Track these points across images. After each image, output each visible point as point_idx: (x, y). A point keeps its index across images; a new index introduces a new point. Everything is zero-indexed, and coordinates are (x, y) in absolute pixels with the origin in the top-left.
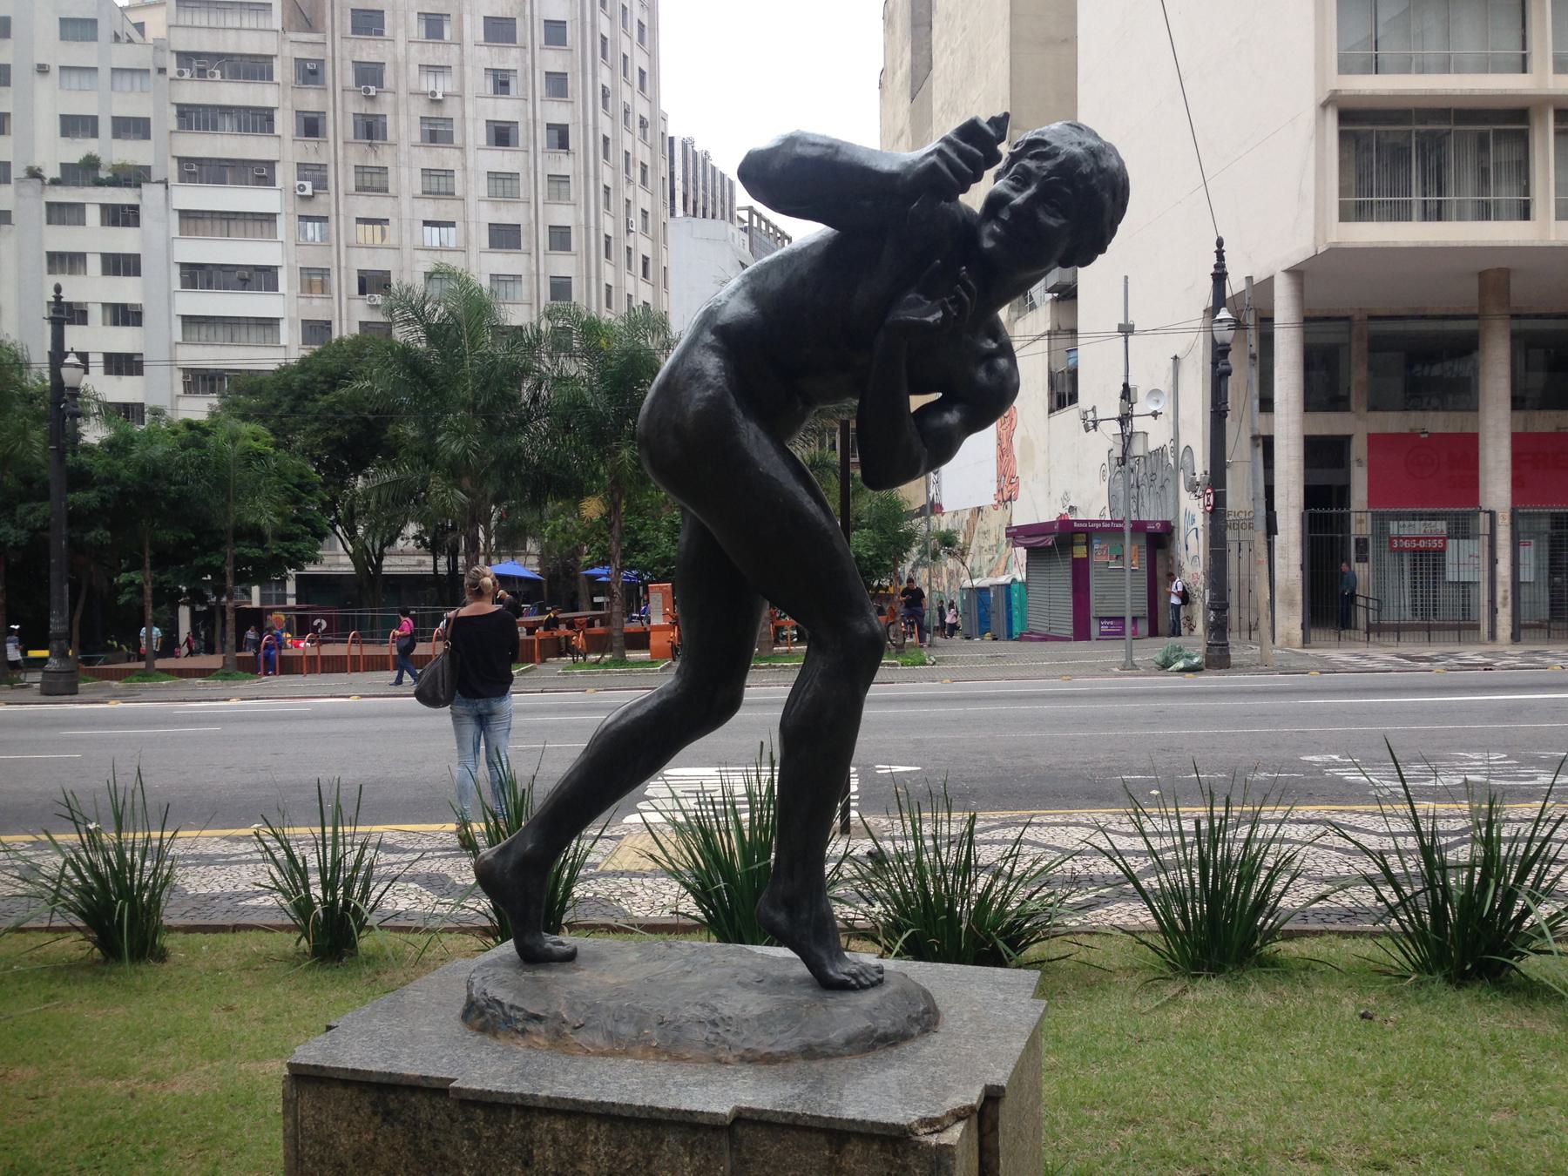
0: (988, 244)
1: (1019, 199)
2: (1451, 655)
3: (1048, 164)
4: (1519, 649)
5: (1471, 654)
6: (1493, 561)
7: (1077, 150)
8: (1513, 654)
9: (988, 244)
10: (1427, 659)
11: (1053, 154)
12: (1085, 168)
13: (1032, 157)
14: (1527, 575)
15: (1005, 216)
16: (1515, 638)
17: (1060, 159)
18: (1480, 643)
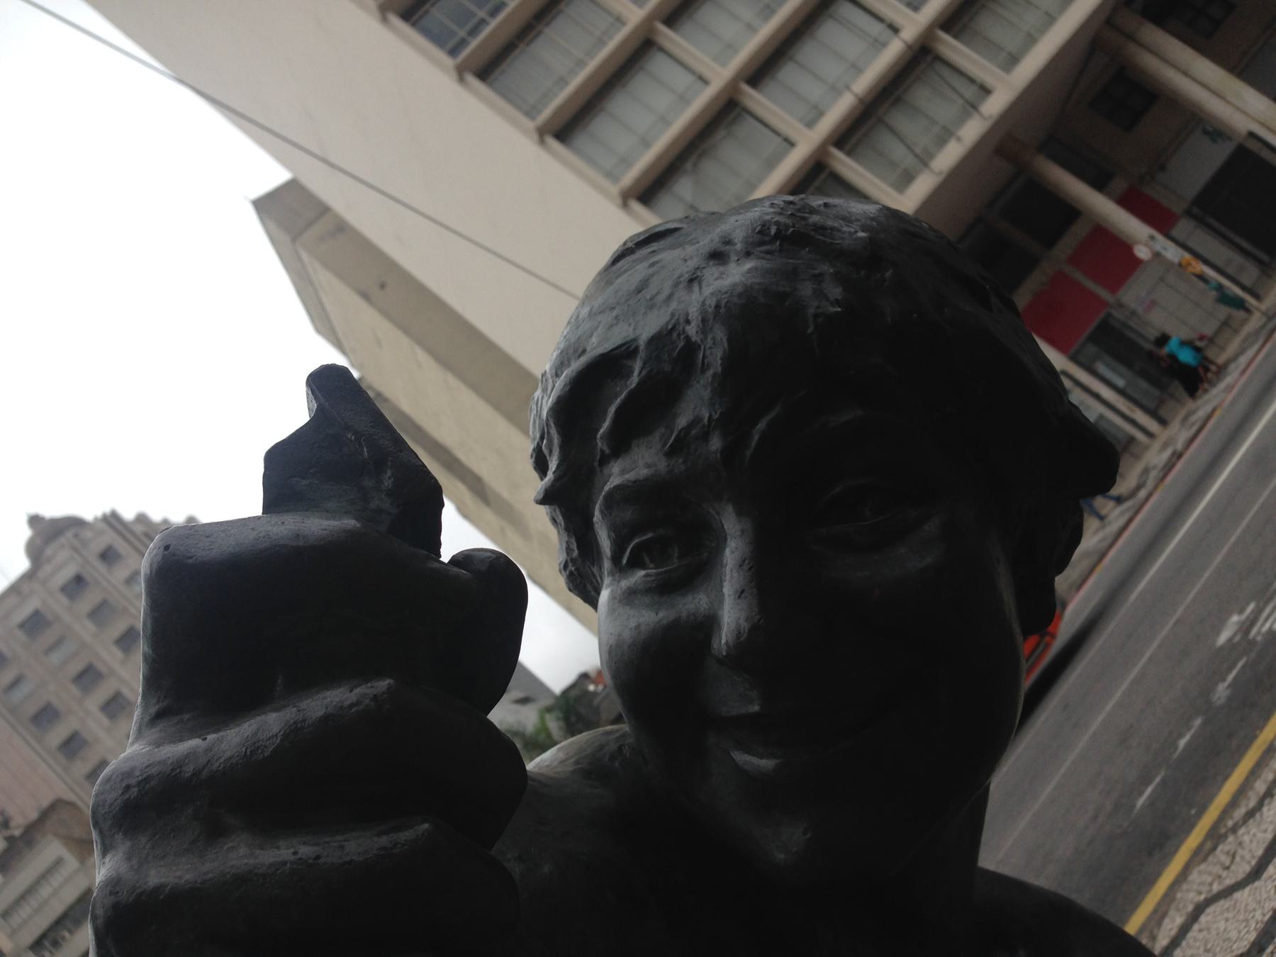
0: (785, 842)
1: (729, 607)
2: (1146, 471)
3: (697, 404)
4: (1175, 425)
5: (1156, 457)
6: (1097, 396)
7: (737, 274)
8: (1178, 433)
9: (785, 842)
10: (1139, 487)
11: (672, 359)
12: (822, 295)
13: (620, 444)
14: (1121, 383)
15: (736, 698)
16: (1163, 422)
17: (715, 353)
18: (1147, 448)
